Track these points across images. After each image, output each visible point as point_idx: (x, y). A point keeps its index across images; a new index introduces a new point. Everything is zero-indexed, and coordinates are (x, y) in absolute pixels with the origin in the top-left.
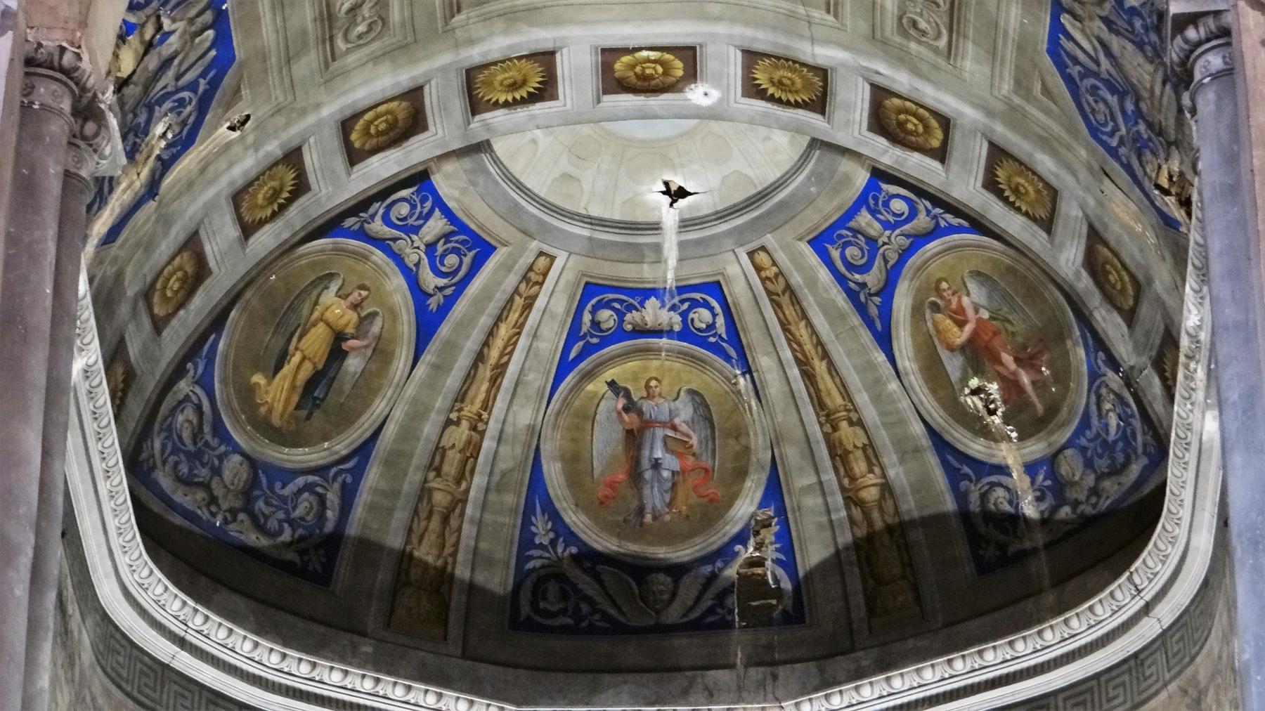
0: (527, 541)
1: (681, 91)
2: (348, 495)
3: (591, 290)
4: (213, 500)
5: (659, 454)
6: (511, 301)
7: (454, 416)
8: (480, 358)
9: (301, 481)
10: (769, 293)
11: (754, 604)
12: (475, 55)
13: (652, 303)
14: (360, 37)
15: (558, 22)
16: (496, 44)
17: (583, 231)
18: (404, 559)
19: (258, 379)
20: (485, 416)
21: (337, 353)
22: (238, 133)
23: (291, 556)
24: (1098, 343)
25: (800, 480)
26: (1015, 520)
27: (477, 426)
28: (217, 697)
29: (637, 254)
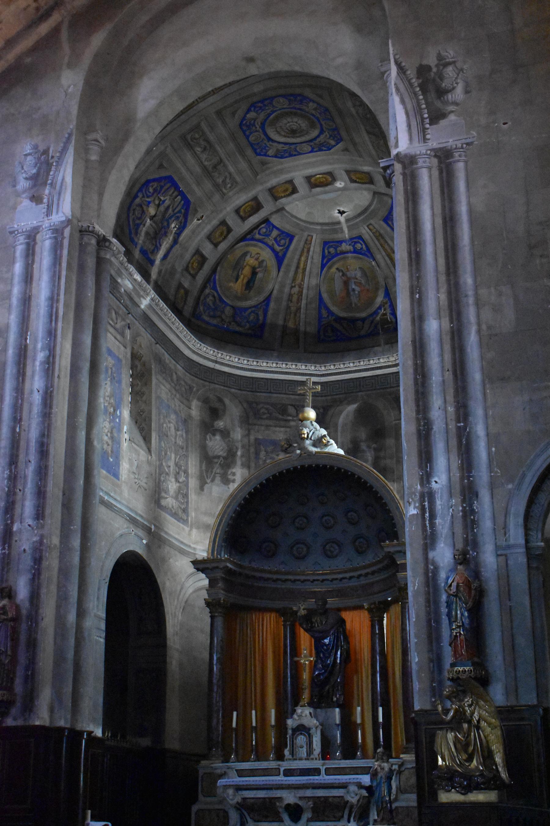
0: (320, 317)
1: (333, 184)
3: (325, 243)
4: (223, 320)
5: (354, 287)
6: (303, 250)
7: (293, 285)
8: (298, 267)
9: (250, 310)
10: (375, 236)
11: (386, 326)
12: (269, 185)
13: (344, 244)
14: (230, 187)
15: (289, 172)
16: (274, 181)
17: (319, 227)
18: (285, 327)
19: (232, 284)
20: (302, 283)
21: (254, 273)
22: (201, 221)
23: (250, 332)
27: (301, 286)
28: (230, 375)
29: (335, 231)
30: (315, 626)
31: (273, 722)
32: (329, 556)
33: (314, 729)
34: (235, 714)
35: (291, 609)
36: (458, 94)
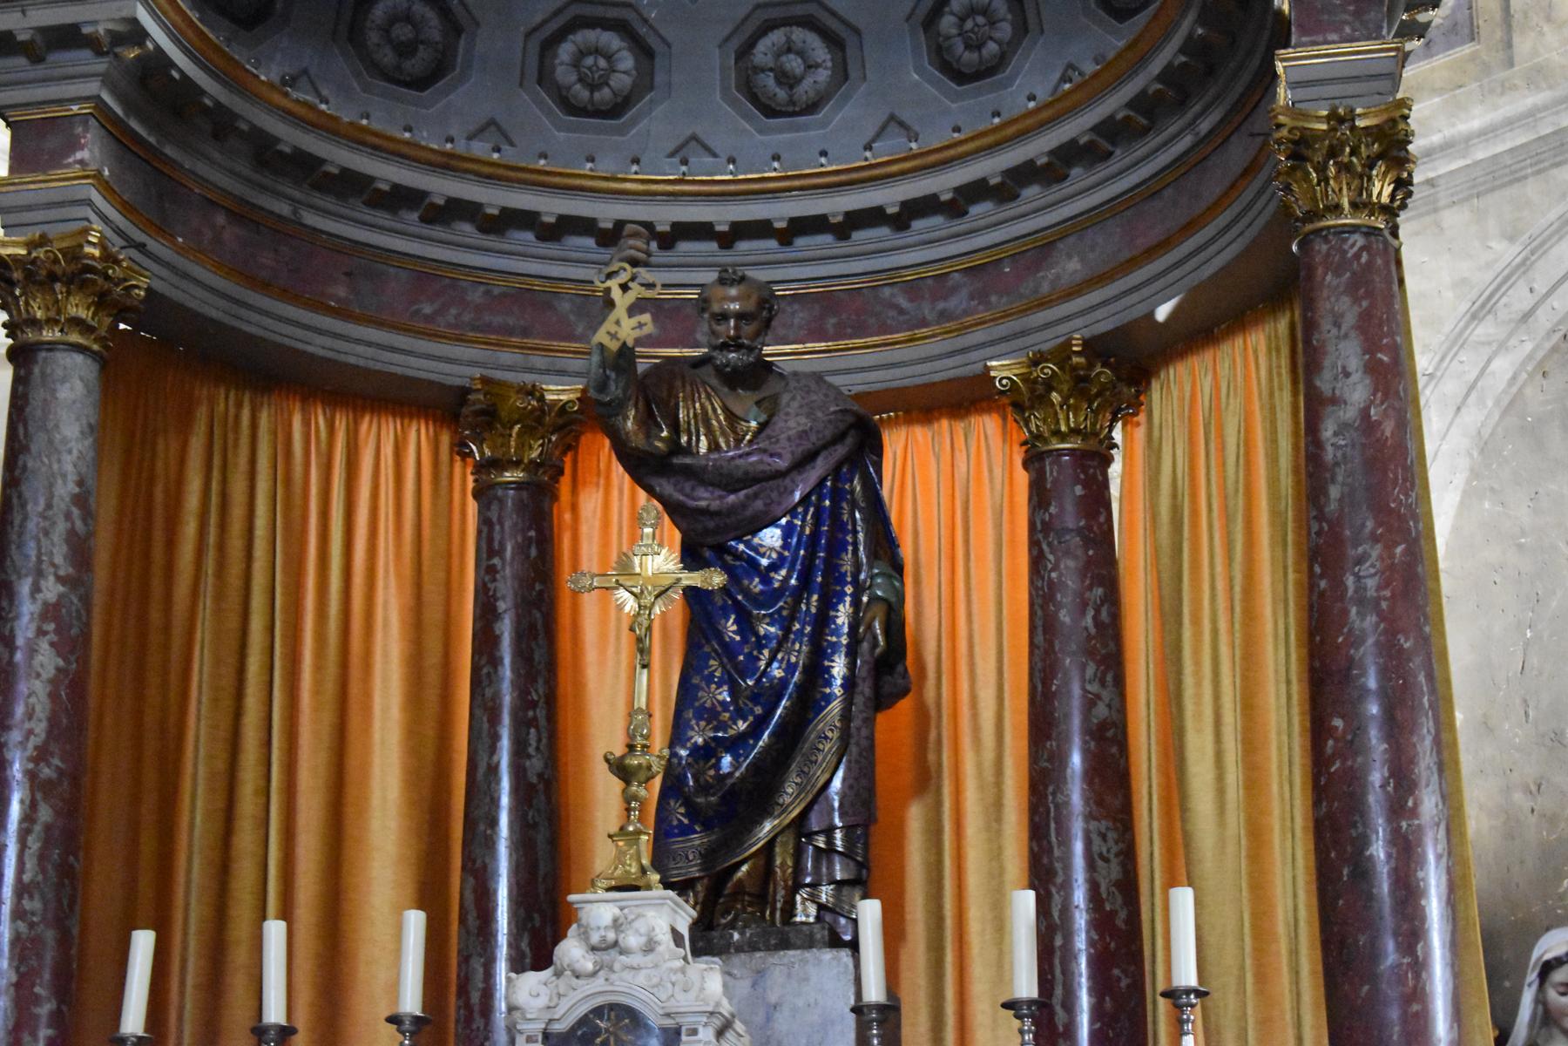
30: (688, 451)
31: (411, 1001)
32: (773, 102)
33: (706, 1034)
34: (143, 943)
35: (533, 391)
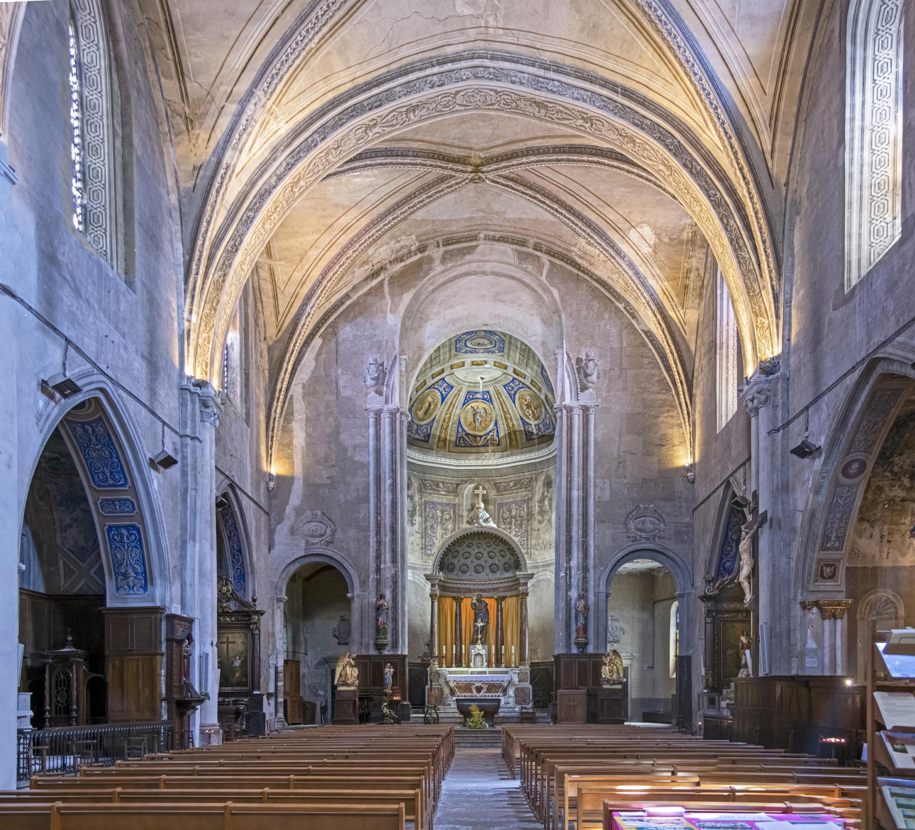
2: (431, 427)
18: (440, 436)
21: (430, 406)
24: (546, 409)
25: (500, 422)
26: (532, 433)
27: (450, 414)
36: (594, 378)
